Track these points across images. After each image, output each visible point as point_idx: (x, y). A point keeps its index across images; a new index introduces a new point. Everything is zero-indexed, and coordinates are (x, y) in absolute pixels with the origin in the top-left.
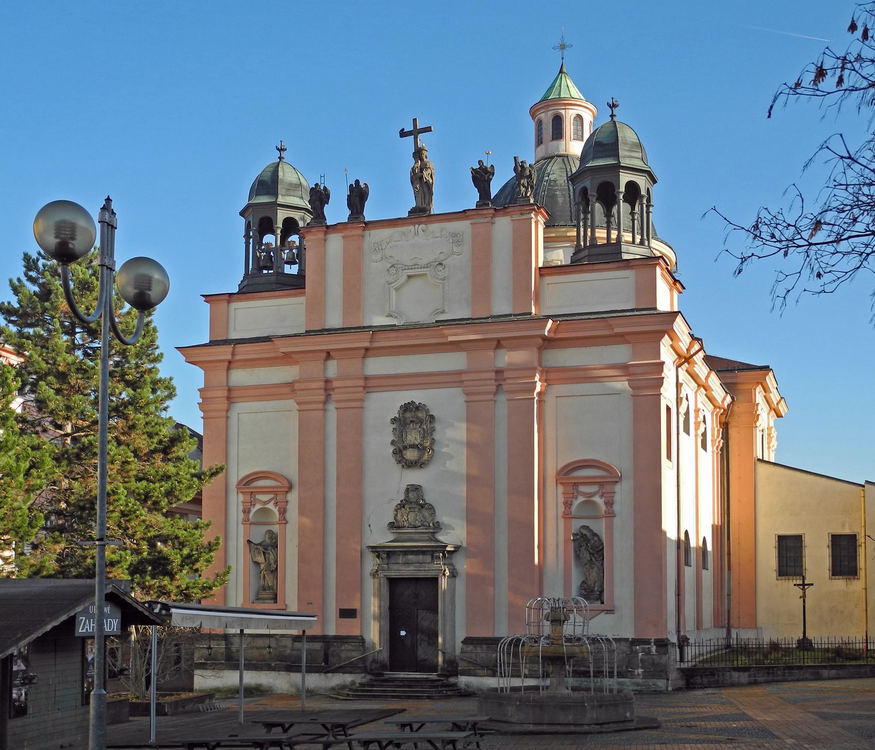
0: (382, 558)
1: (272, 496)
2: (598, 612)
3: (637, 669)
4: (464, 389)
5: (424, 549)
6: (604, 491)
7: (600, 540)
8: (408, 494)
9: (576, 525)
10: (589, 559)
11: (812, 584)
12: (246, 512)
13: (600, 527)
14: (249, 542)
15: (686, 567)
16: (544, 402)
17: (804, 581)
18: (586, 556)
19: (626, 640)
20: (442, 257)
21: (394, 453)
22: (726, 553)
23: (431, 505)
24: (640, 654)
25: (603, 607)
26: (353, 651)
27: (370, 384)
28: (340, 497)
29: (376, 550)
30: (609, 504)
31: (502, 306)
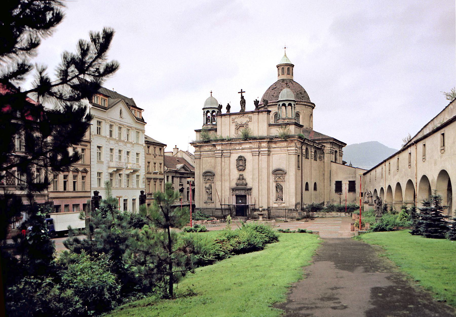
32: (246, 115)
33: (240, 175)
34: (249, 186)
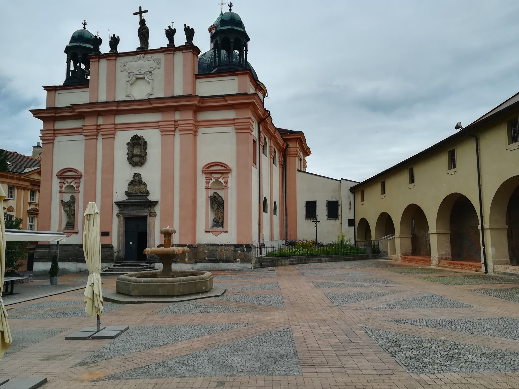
0: (121, 208)
1: (73, 179)
2: (221, 232)
3: (238, 259)
4: (160, 129)
5: (141, 203)
6: (223, 176)
7: (222, 199)
8: (134, 178)
9: (211, 193)
10: (217, 207)
11: (320, 221)
12: (61, 187)
13: (221, 193)
14: (62, 201)
15: (264, 213)
16: (197, 135)
17: (316, 220)
18: (216, 206)
19: (233, 245)
20: (151, 70)
21: (128, 159)
22: (285, 209)
23: (145, 183)
24: (239, 252)
25: (223, 230)
26: (107, 252)
27: (117, 127)
28: (103, 179)
29: (119, 204)
30: (226, 182)
31: (178, 91)
32: (149, 56)
33: (137, 175)
34: (151, 198)
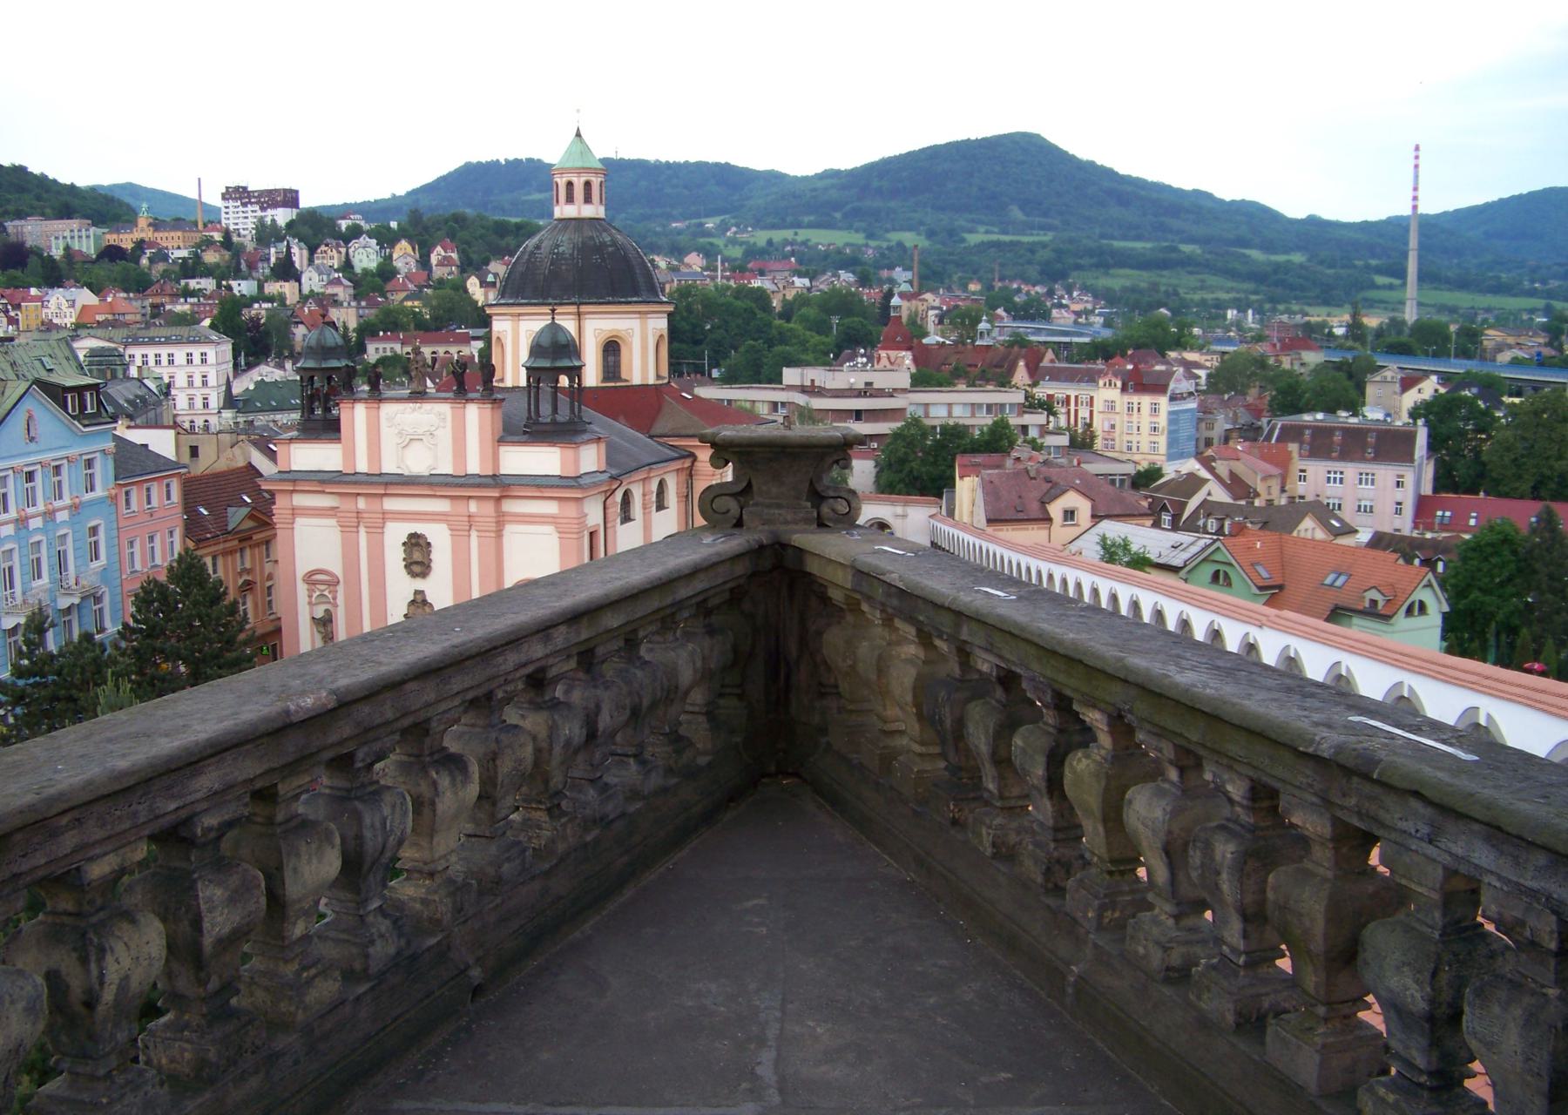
12: (310, 597)
27: (386, 516)
31: (474, 467)
33: (417, 592)
